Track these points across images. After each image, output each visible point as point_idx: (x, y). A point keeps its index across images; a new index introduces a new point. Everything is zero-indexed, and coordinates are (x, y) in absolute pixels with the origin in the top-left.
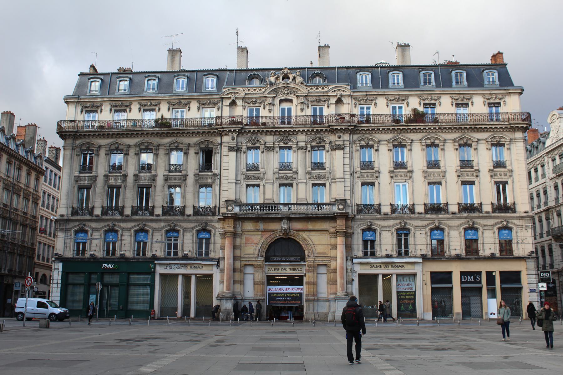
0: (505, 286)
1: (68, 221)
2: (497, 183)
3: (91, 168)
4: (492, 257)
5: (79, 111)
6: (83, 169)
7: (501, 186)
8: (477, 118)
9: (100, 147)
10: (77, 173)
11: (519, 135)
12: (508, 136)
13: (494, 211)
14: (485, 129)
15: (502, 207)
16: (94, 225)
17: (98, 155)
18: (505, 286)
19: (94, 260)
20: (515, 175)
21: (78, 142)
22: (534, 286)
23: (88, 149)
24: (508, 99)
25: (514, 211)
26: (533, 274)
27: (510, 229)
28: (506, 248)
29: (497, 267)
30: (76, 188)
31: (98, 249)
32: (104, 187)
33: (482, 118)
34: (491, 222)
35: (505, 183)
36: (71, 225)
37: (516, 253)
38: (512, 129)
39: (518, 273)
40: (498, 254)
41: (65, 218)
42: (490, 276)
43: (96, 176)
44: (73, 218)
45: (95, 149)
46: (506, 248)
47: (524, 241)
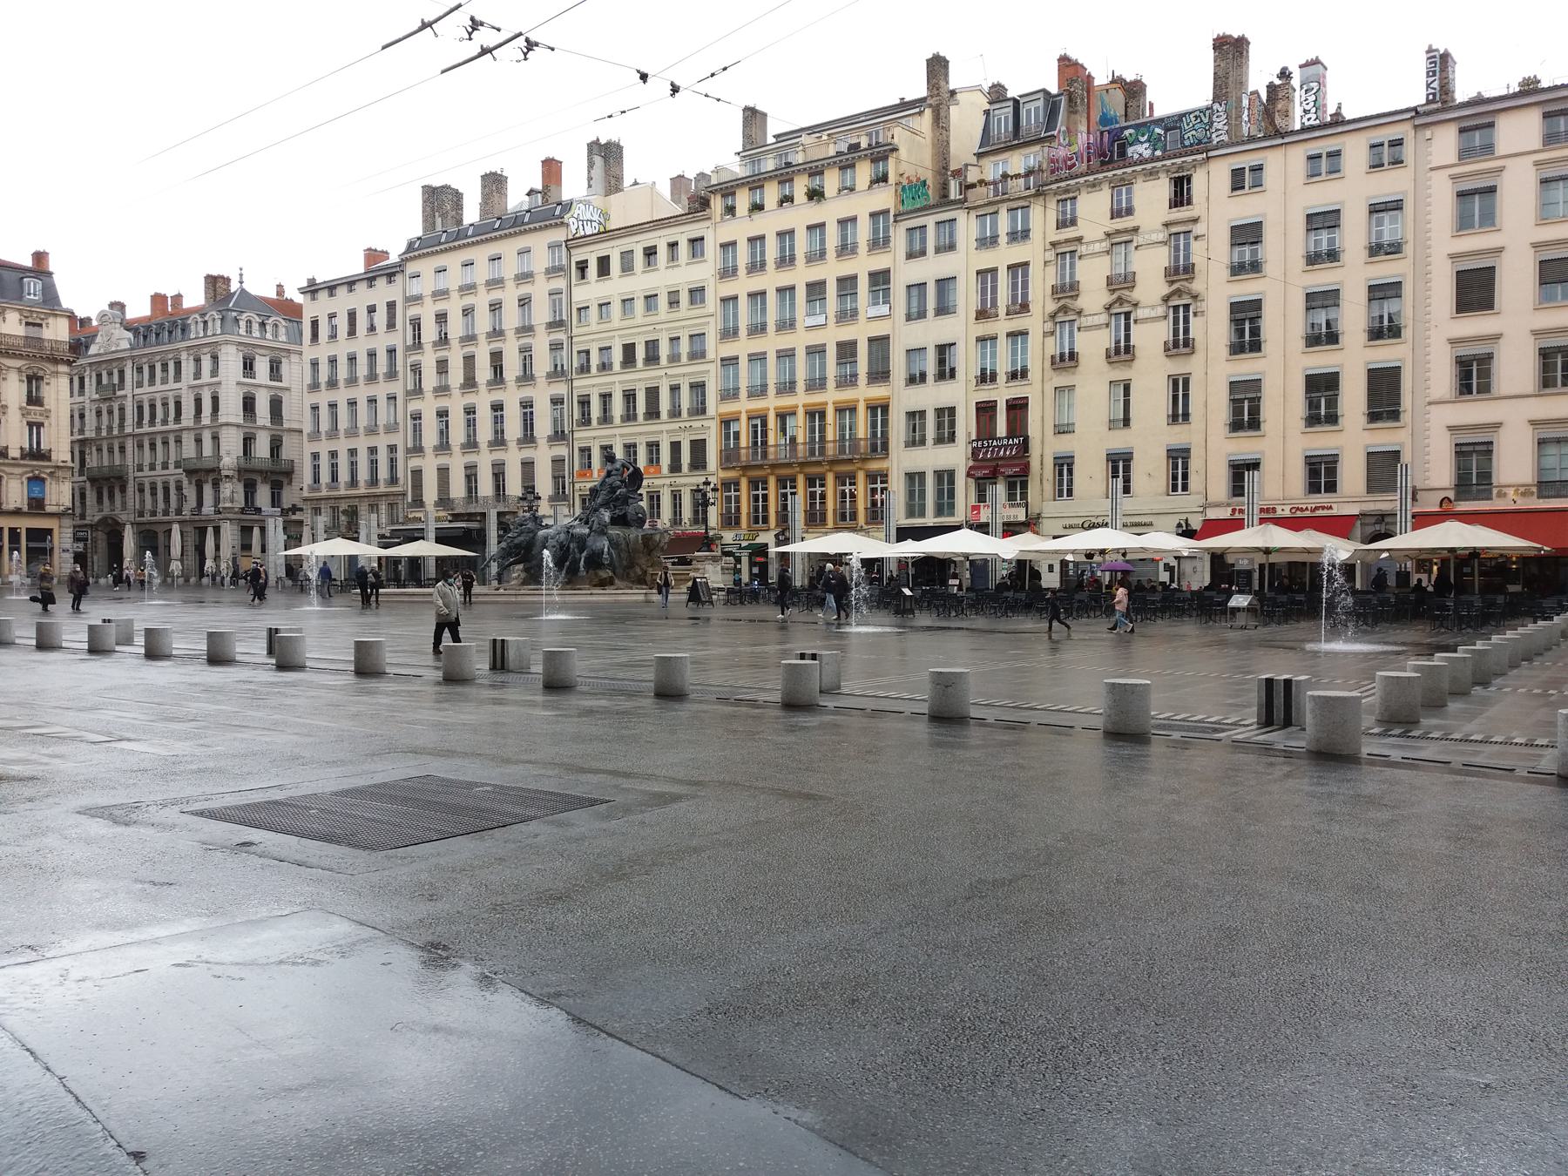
0: (32, 545)
2: (30, 425)
4: (17, 512)
7: (35, 426)
8: (11, 341)
11: (63, 368)
12: (50, 367)
13: (23, 457)
14: (21, 357)
15: (36, 454)
18: (32, 545)
20: (53, 415)
22: (68, 546)
24: (51, 320)
25: (49, 459)
26: (68, 533)
27: (43, 480)
28: (37, 505)
29: (23, 524)
33: (16, 342)
34: (20, 470)
35: (40, 425)
37: (49, 509)
38: (55, 361)
39: (50, 531)
40: (25, 509)
42: (14, 533)
46: (37, 505)
47: (60, 494)
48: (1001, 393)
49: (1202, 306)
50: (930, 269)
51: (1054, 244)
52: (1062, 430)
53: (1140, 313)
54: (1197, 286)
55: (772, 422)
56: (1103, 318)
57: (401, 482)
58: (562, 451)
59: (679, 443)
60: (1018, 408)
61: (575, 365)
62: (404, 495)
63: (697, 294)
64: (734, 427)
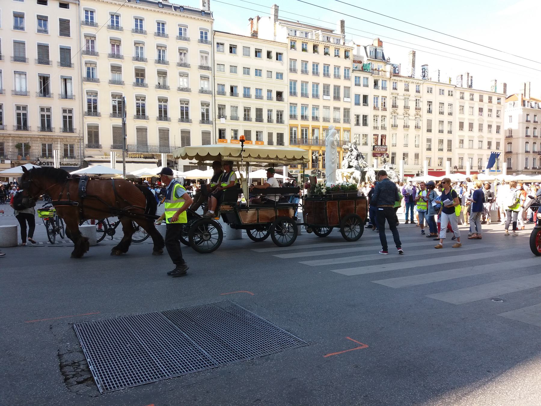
48: (380, 132)
49: (421, 118)
50: (362, 91)
51: (392, 94)
52: (394, 145)
53: (410, 117)
54: (421, 113)
55: (310, 131)
56: (402, 117)
57: (78, 131)
58: (207, 127)
59: (250, 132)
60: (384, 137)
61: (216, 90)
62: (82, 139)
63: (280, 76)
64: (294, 129)
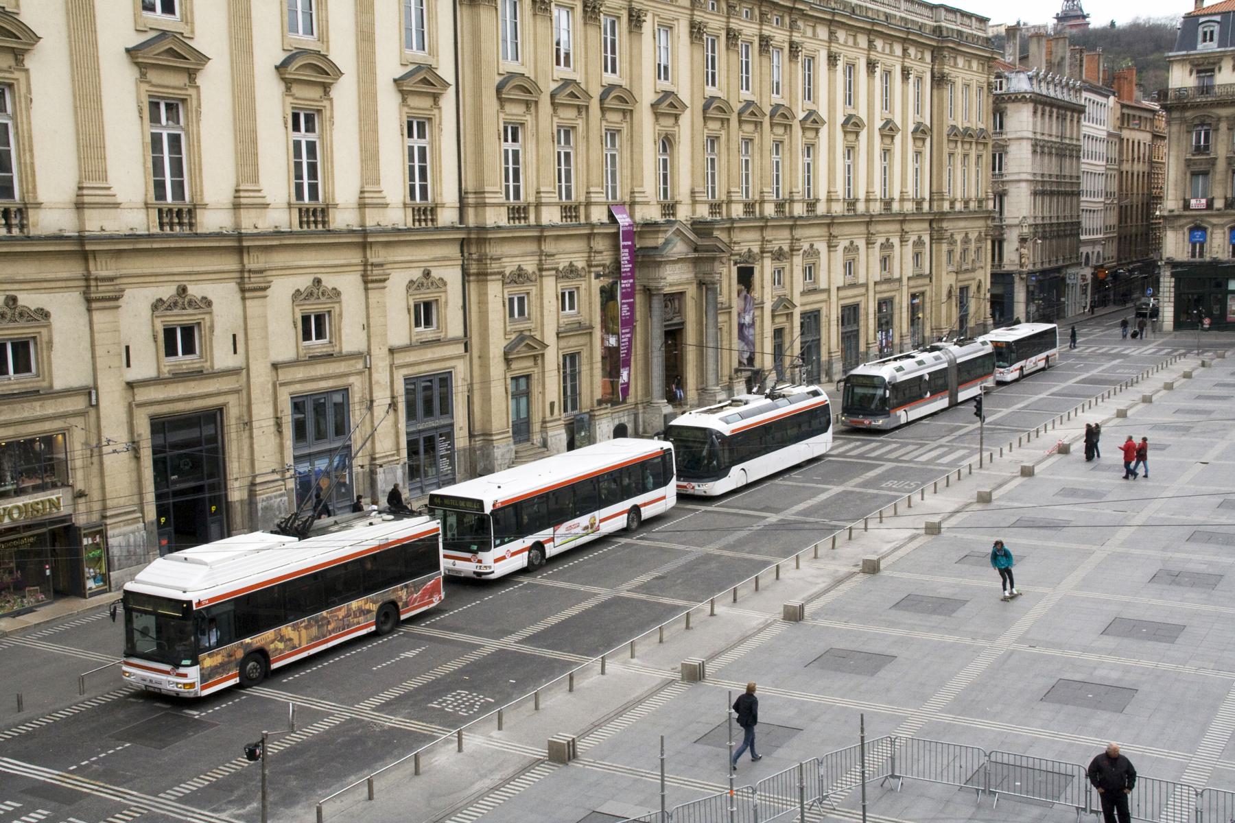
1: (1179, 217)
3: (1207, 147)
5: (1187, 72)
6: (1198, 150)
9: (1219, 119)
10: (1189, 156)
16: (1215, 221)
17: (1217, 130)
19: (1215, 264)
21: (1189, 114)
23: (1202, 124)
30: (1188, 175)
31: (1220, 250)
32: (1227, 172)
36: (1183, 221)
41: (1176, 213)
43: (1216, 159)
44: (1187, 213)
45: (1214, 123)
